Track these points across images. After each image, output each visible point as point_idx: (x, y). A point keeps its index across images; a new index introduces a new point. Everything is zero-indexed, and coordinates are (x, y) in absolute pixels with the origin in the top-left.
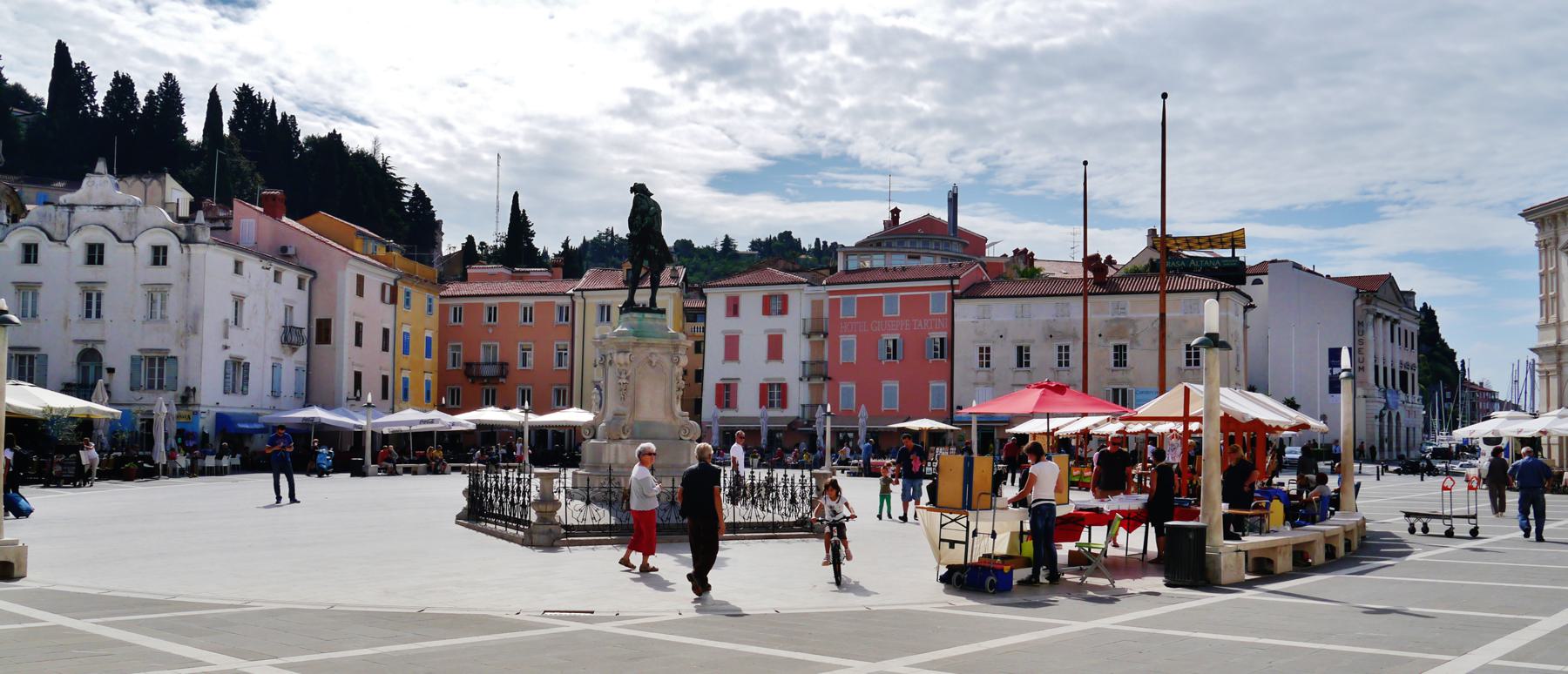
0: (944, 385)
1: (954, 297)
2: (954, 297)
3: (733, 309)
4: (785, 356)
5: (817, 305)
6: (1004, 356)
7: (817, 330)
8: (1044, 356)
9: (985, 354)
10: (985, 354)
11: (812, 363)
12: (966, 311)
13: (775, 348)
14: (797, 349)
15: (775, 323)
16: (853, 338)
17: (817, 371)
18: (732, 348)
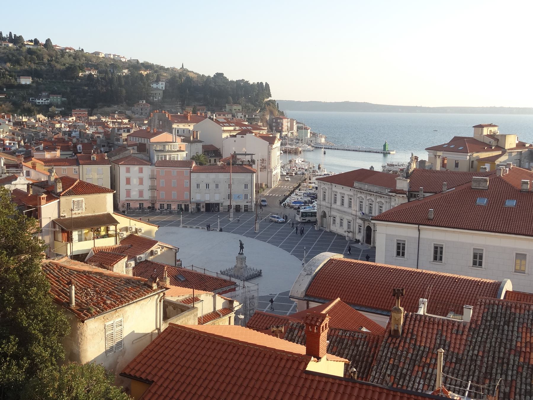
0: (188, 193)
1: (191, 172)
2: (191, 172)
3: (128, 171)
4: (144, 184)
5: (152, 171)
6: (203, 186)
7: (152, 178)
8: (212, 186)
9: (198, 186)
10: (198, 186)
11: (152, 186)
12: (194, 175)
13: (141, 182)
14: (147, 183)
15: (141, 175)
16: (164, 180)
17: (153, 188)
18: (128, 181)
